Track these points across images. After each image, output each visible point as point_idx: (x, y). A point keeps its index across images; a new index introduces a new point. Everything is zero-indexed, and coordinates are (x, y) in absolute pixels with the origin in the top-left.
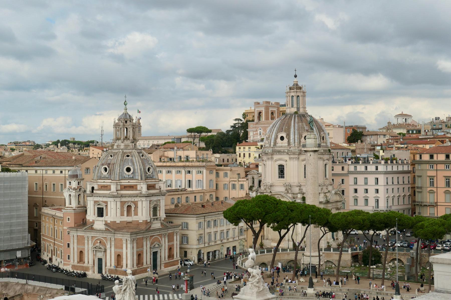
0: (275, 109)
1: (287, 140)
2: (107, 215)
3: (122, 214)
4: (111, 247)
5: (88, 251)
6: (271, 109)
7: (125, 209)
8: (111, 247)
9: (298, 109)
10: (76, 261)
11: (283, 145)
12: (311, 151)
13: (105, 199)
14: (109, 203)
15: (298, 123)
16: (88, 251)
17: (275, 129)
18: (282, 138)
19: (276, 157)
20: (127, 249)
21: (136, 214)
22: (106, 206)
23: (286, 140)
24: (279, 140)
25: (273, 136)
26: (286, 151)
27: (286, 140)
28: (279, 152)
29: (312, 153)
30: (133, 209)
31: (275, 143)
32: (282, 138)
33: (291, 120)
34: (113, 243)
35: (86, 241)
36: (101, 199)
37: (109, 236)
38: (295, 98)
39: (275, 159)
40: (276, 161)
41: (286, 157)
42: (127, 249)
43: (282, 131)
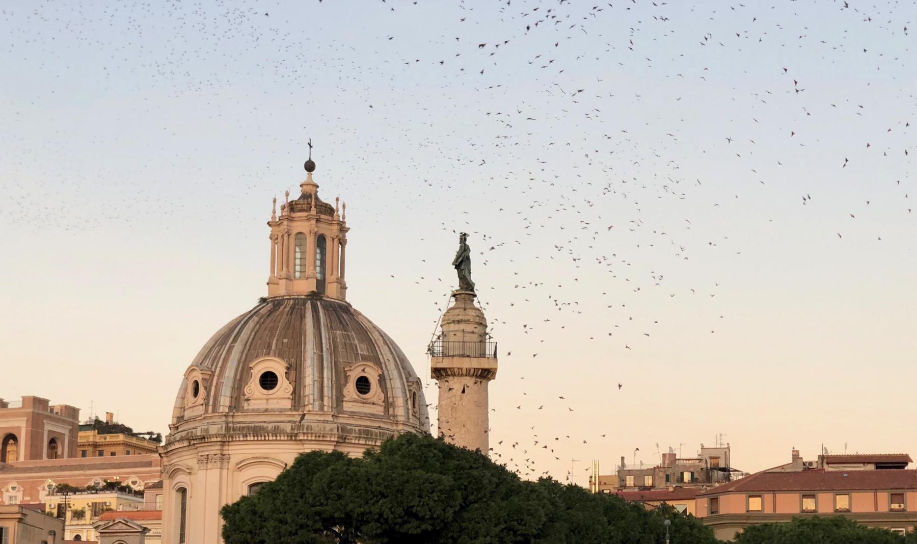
0: (64, 430)
1: (291, 388)
6: (48, 427)
9: (321, 284)
11: (273, 404)
12: (468, 373)
15: (331, 328)
17: (238, 347)
18: (268, 381)
19: (239, 451)
23: (284, 386)
24: (253, 387)
25: (230, 372)
26: (289, 430)
27: (284, 386)
28: (257, 432)
29: (469, 381)
32: (268, 381)
33: (302, 317)
38: (311, 242)
39: (234, 460)
40: (240, 466)
43: (268, 354)
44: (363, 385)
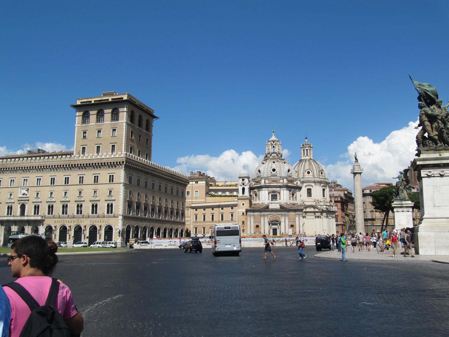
2: (280, 199)
3: (290, 199)
4: (285, 220)
5: (264, 224)
7: (291, 196)
8: (285, 220)
10: (253, 232)
11: (310, 177)
13: (278, 189)
14: (282, 192)
16: (264, 224)
18: (309, 173)
19: (305, 184)
20: (299, 220)
21: (296, 200)
22: (279, 193)
30: (295, 196)
31: (303, 175)
32: (309, 173)
34: (287, 218)
35: (262, 218)
36: (275, 189)
37: (283, 213)
41: (313, 184)
42: (299, 220)
44: (322, 173)
